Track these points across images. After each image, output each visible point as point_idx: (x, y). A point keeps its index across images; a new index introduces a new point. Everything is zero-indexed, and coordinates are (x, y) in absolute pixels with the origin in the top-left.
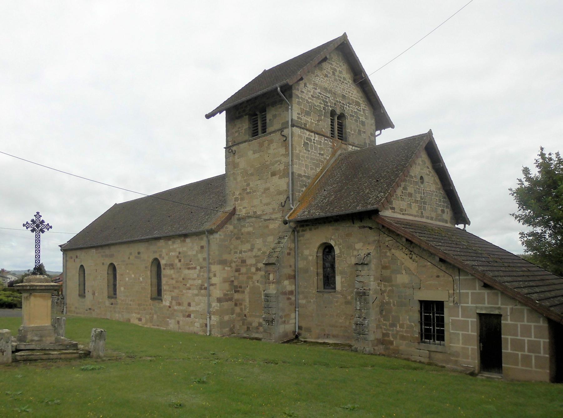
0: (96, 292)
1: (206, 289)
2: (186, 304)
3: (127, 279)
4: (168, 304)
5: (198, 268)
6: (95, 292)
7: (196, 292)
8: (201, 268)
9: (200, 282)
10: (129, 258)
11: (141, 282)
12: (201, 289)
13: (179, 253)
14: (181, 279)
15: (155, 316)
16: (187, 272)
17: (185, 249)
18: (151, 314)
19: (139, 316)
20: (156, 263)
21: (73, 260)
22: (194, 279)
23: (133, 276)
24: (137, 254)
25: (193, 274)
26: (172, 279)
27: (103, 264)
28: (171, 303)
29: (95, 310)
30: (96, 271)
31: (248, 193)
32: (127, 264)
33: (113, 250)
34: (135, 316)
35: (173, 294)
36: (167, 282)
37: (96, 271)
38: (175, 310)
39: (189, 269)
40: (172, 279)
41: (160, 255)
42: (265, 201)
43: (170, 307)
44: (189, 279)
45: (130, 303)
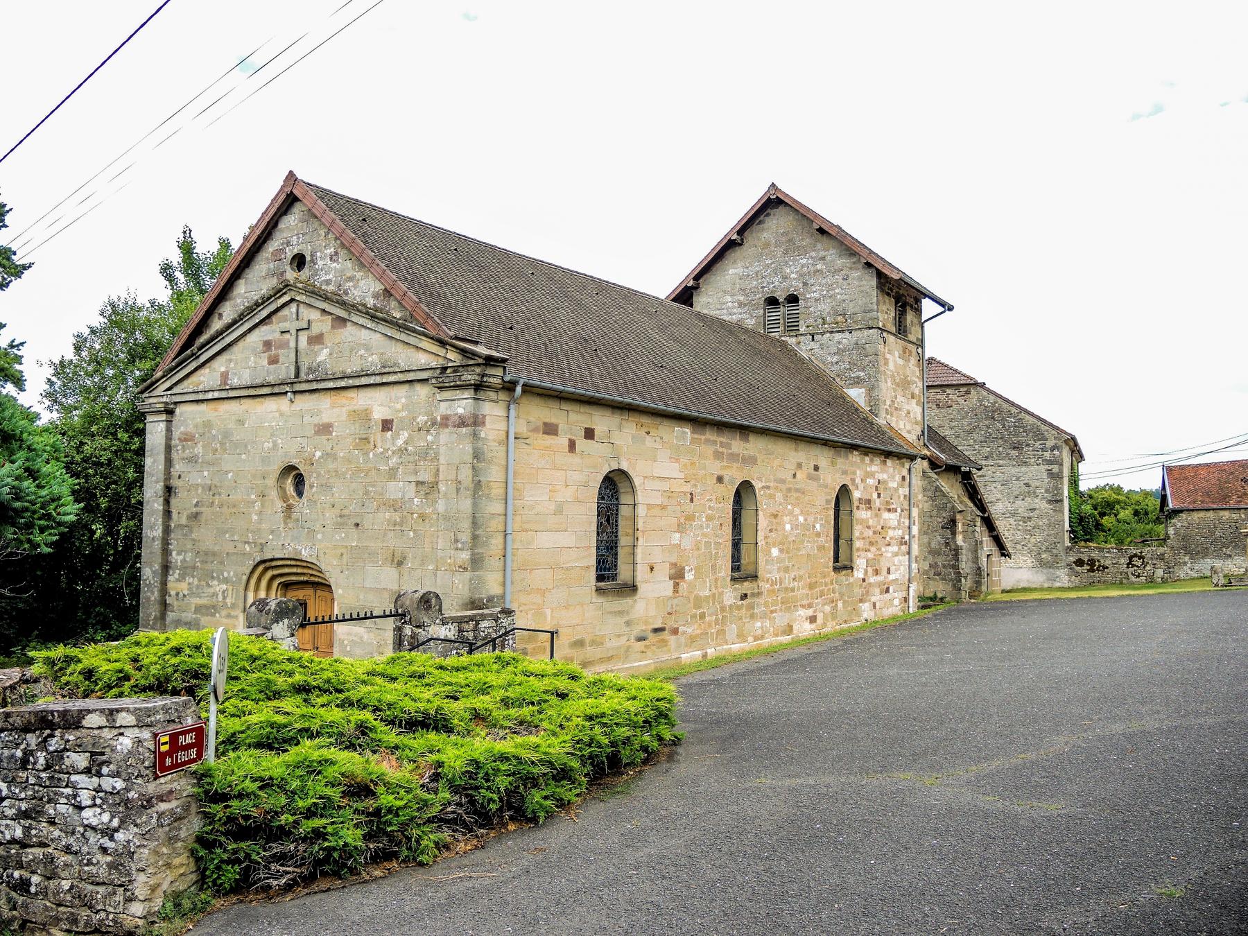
0: (687, 568)
1: (906, 543)
2: (884, 572)
3: (788, 527)
4: (861, 576)
5: (899, 510)
6: (683, 569)
7: (895, 549)
8: (902, 511)
9: (900, 533)
10: (795, 475)
11: (818, 535)
12: (901, 544)
13: (879, 481)
14: (879, 528)
15: (840, 604)
16: (886, 515)
17: (885, 476)
18: (833, 602)
19: (810, 612)
20: (844, 492)
21: (562, 441)
22: (894, 528)
23: (801, 519)
24: (812, 470)
25: (892, 519)
26: (868, 527)
27: (720, 479)
28: (866, 572)
29: (681, 629)
30: (692, 500)
31: (896, 409)
32: (789, 490)
33: (755, 446)
34: (802, 614)
35: (870, 555)
36: (862, 533)
37: (692, 500)
38: (870, 584)
39: (889, 510)
40: (868, 527)
41: (853, 480)
42: (908, 427)
43: (864, 580)
44: (890, 528)
45: (792, 585)
